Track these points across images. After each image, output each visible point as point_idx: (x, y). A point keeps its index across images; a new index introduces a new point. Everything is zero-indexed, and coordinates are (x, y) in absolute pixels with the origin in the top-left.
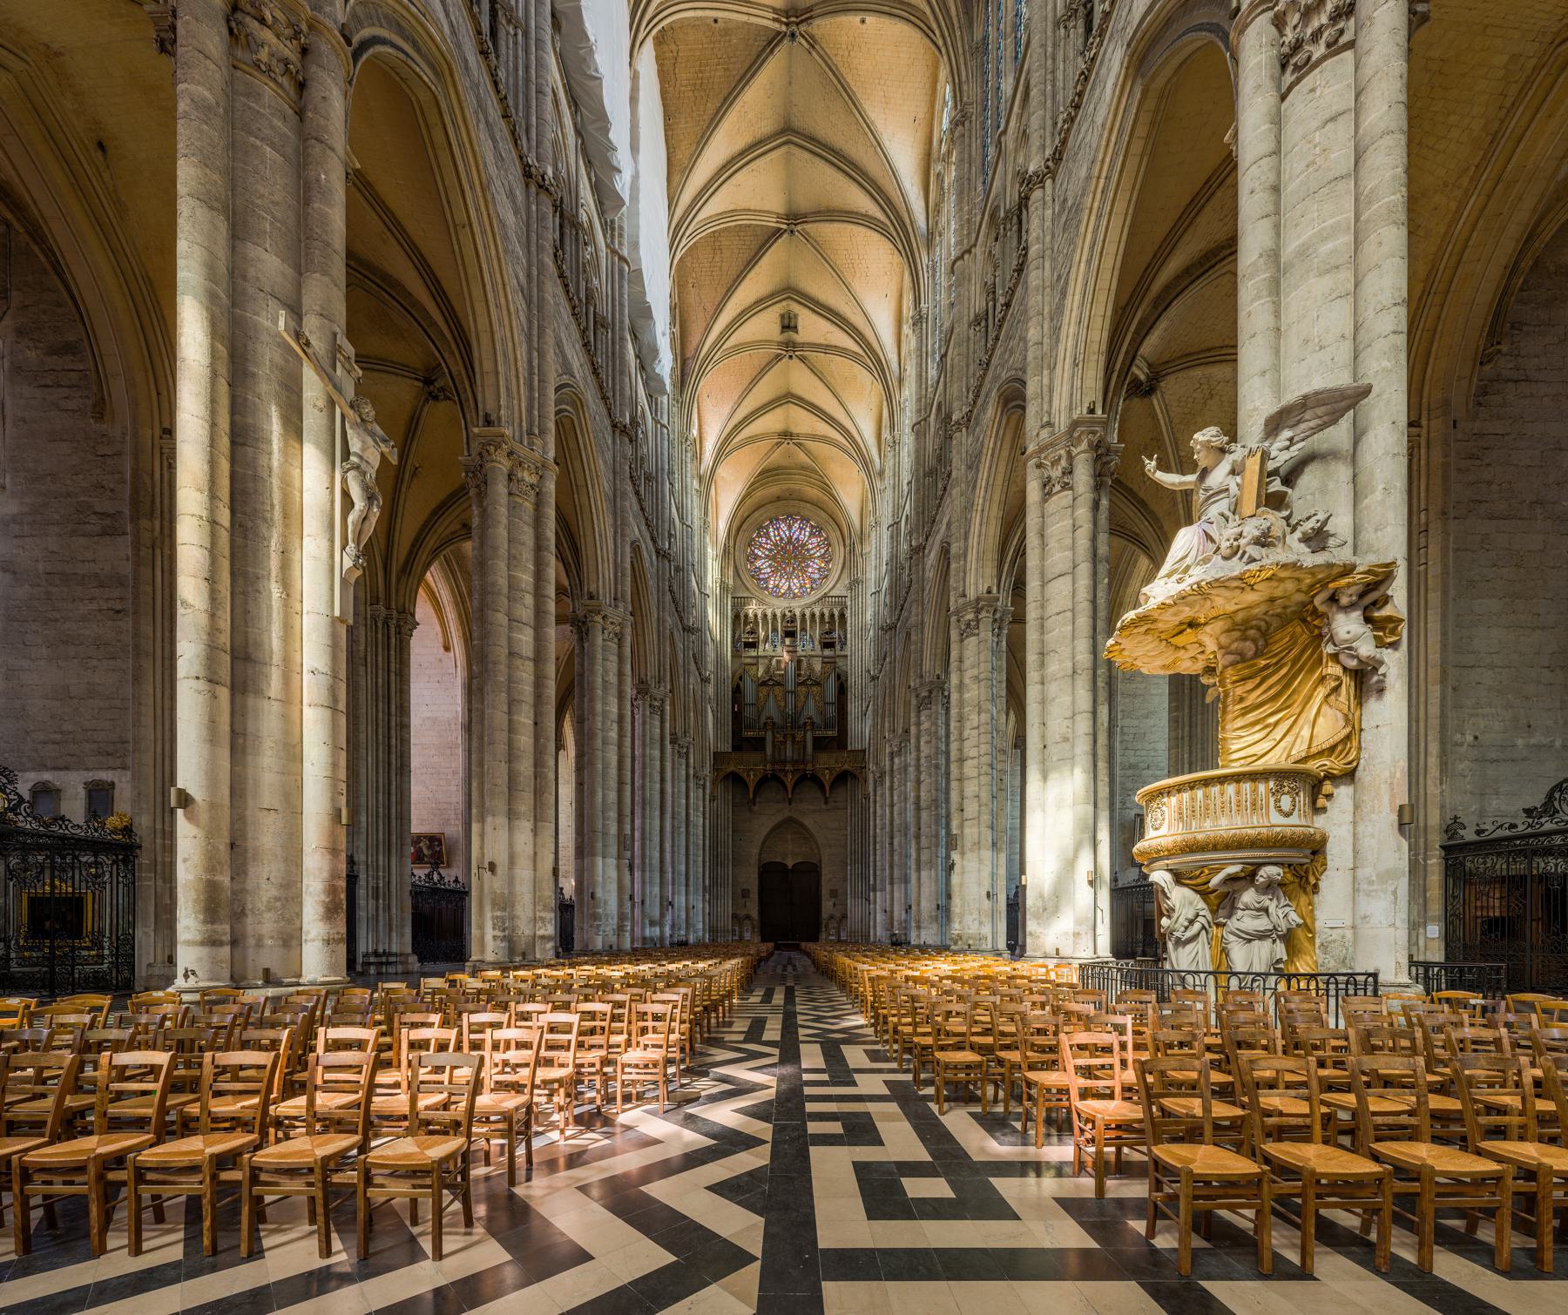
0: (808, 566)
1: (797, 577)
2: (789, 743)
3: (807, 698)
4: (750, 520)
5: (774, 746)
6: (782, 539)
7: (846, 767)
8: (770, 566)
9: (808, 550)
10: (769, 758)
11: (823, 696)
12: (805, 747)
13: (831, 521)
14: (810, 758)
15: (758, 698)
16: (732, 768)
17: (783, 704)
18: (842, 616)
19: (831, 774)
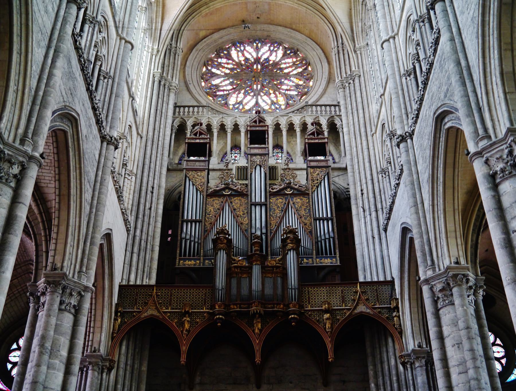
0: (282, 84)
1: (268, 94)
2: (256, 270)
3: (285, 211)
4: (207, 41)
5: (230, 273)
6: (247, 60)
7: (362, 308)
8: (231, 84)
9: (281, 69)
10: (220, 294)
11: (310, 209)
12: (284, 275)
13: (309, 41)
14: (293, 293)
15: (205, 212)
16: (151, 312)
17: (246, 221)
18: (333, 128)
19: (333, 319)
